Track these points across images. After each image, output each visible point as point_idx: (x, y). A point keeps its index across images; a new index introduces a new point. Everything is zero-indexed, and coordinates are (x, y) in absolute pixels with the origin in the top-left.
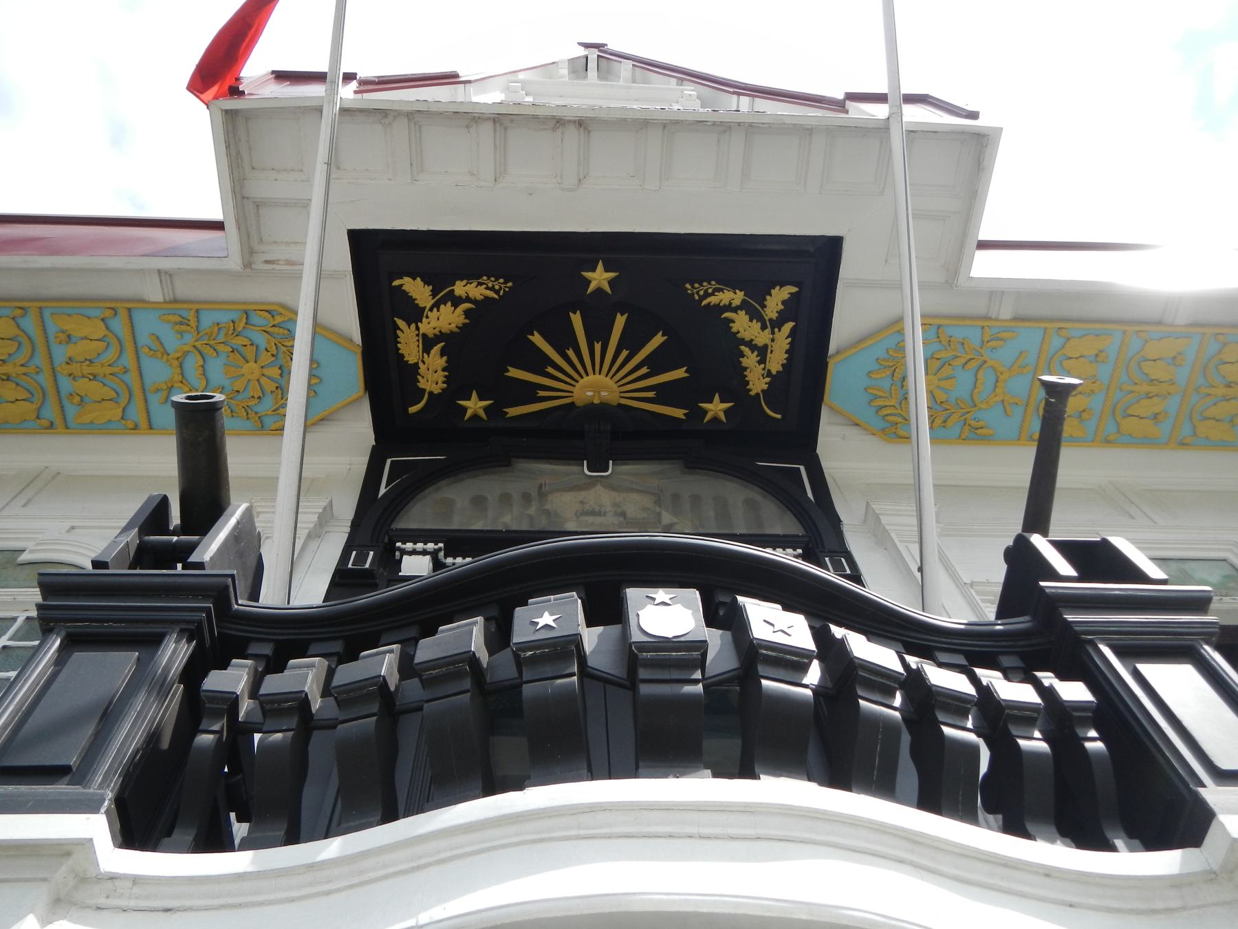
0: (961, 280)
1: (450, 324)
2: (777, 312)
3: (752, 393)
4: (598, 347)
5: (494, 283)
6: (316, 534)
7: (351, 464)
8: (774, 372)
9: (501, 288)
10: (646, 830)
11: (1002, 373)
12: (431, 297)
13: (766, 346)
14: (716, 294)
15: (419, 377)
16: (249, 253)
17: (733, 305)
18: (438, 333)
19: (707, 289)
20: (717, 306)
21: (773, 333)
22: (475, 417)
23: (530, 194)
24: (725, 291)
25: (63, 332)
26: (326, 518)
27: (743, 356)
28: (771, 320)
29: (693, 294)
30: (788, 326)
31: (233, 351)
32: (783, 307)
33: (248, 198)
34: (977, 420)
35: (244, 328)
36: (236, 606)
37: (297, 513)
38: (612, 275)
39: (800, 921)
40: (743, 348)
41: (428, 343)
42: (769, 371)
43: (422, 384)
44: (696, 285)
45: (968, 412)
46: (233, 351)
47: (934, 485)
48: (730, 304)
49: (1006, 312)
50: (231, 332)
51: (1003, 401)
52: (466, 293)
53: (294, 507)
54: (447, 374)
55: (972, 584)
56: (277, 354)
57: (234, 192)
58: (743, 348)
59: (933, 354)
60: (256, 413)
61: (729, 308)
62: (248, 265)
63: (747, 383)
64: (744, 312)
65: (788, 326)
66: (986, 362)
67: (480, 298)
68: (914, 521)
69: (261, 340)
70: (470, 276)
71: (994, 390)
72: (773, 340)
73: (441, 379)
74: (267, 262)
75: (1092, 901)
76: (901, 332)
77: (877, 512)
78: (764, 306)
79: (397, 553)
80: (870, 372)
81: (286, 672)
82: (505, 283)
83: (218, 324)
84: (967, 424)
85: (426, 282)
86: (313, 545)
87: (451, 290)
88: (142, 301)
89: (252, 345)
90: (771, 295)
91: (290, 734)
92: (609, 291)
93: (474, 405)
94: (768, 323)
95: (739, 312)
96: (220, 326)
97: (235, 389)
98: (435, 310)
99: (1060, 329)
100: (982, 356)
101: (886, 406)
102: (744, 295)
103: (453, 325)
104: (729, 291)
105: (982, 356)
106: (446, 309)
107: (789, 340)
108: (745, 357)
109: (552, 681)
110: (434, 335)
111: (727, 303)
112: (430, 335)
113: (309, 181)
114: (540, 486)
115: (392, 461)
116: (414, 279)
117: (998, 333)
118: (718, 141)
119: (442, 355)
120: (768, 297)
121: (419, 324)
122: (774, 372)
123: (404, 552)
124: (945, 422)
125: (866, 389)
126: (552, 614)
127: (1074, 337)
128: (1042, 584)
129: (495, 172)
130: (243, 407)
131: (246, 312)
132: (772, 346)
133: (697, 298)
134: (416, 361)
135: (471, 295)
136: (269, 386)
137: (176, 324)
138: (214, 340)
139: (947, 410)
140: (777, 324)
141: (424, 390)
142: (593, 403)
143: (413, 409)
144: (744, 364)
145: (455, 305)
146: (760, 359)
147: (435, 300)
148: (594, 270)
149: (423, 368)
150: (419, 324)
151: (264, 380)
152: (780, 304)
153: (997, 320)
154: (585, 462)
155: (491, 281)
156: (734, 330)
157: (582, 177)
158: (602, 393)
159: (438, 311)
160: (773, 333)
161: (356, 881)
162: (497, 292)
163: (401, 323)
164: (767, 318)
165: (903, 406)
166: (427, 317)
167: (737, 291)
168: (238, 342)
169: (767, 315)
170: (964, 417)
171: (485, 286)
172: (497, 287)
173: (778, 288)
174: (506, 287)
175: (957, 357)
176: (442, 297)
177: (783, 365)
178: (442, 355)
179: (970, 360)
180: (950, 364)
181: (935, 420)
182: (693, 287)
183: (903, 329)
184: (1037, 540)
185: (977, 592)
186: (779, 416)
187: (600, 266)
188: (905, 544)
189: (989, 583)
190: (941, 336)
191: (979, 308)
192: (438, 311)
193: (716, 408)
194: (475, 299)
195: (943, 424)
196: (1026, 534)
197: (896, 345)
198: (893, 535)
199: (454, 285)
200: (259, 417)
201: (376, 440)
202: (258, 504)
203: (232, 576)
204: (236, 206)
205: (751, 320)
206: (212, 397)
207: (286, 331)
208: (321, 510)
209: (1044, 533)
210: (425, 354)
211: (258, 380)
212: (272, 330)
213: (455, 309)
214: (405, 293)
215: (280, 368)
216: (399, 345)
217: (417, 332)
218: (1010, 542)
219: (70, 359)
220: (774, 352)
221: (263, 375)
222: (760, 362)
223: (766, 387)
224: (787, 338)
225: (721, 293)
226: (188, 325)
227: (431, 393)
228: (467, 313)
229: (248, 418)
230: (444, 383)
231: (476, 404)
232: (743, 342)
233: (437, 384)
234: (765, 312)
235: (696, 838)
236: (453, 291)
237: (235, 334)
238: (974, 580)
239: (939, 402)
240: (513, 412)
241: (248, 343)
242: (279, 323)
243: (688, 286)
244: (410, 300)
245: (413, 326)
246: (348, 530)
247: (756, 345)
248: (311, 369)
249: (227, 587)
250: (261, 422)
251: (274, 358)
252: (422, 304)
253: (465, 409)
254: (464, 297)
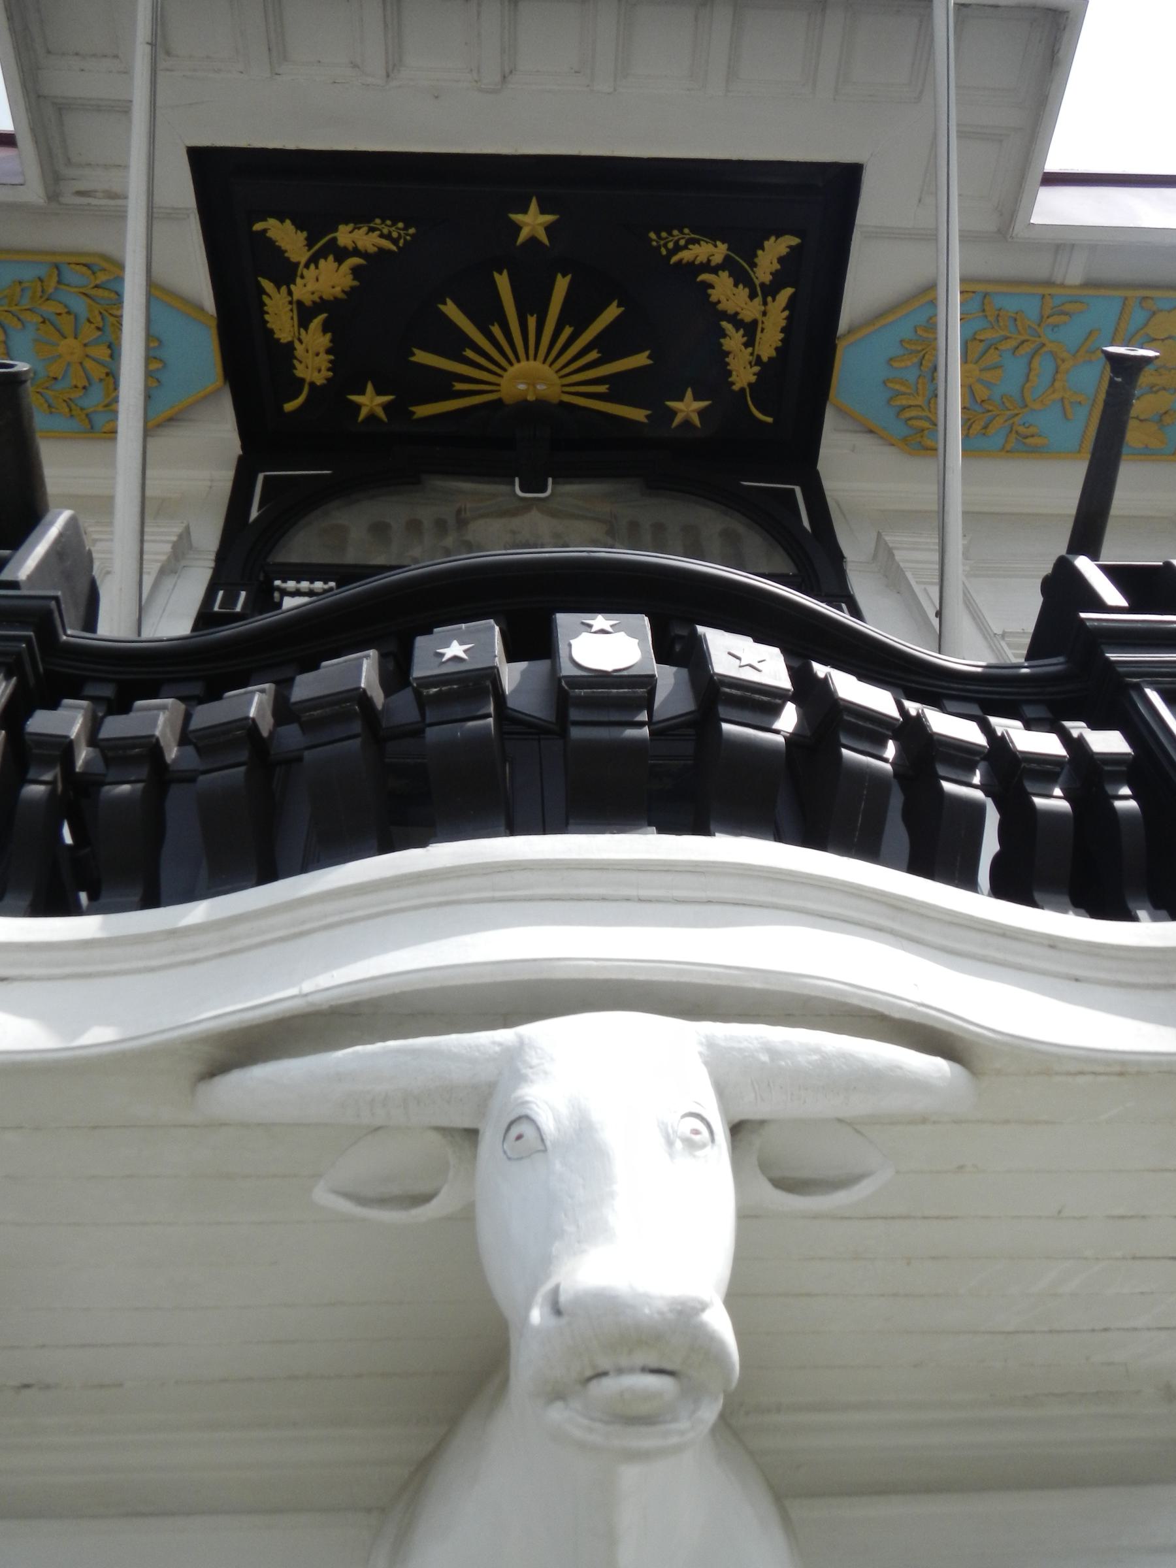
0: (1018, 228)
1: (333, 287)
2: (771, 274)
3: (736, 388)
4: (532, 321)
6: (169, 569)
7: (212, 480)
8: (765, 359)
9: (400, 236)
10: (574, 891)
11: (1063, 361)
12: (306, 248)
13: (755, 323)
14: (690, 246)
15: (295, 362)
16: (54, 179)
17: (713, 264)
18: (318, 300)
19: (679, 239)
20: (691, 264)
21: (765, 303)
22: (372, 417)
23: (437, 97)
24: (702, 243)
26: (182, 549)
27: (725, 335)
28: (762, 285)
29: (659, 247)
30: (786, 293)
31: (44, 322)
32: (778, 267)
33: (45, 97)
34: (1027, 425)
35: (56, 289)
36: (65, 638)
37: (142, 541)
38: (549, 218)
39: (754, 990)
40: (724, 324)
41: (305, 314)
42: (759, 357)
43: (300, 371)
44: (664, 234)
45: (1017, 415)
46: (44, 322)
47: (965, 513)
48: (709, 261)
49: (1074, 272)
50: (39, 294)
51: (1062, 399)
52: (354, 242)
53: (137, 527)
54: (332, 357)
55: (1004, 635)
56: (104, 326)
57: (24, 85)
58: (724, 324)
59: (975, 333)
60: (82, 409)
61: (707, 267)
62: (53, 196)
63: (730, 373)
64: (726, 274)
65: (786, 293)
66: (1044, 345)
67: (372, 250)
68: (936, 557)
69: (80, 306)
70: (360, 218)
71: (1053, 384)
72: (764, 314)
73: (325, 365)
74: (80, 193)
75: (1103, 975)
76: (933, 303)
77: (891, 545)
78: (753, 265)
79: (277, 595)
80: (891, 359)
81: (132, 714)
82: (406, 228)
83: (20, 283)
84: (1014, 432)
85: (299, 227)
86: (168, 582)
89: (69, 313)
90: (763, 250)
91: (140, 786)
92: (546, 241)
93: (370, 401)
94: (759, 289)
95: (720, 273)
96: (24, 285)
97: (52, 375)
98: (312, 266)
99: (1145, 298)
100: (1040, 337)
101: (910, 406)
102: (729, 249)
103: (338, 289)
104: (707, 242)
105: (1040, 337)
106: (327, 265)
107: (786, 313)
108: (728, 338)
109: (463, 724)
110: (314, 302)
111: (705, 261)
112: (308, 303)
113: (127, 72)
114: (459, 512)
115: (266, 477)
116: (282, 221)
117: (1063, 304)
118: (696, 19)
119: (325, 331)
120: (760, 252)
121: (292, 287)
122: (765, 359)
123: (285, 593)
124: (986, 427)
125: (884, 383)
126: (461, 643)
127: (1161, 311)
128: (1083, 615)
129: (387, 62)
130: (65, 401)
131: (57, 266)
132: (763, 322)
133: (664, 252)
134: (290, 339)
135: (360, 245)
136: (97, 372)
138: (16, 305)
139: (989, 411)
140: (770, 291)
141: (302, 381)
142: (526, 401)
143: (289, 407)
144: (725, 348)
145: (340, 260)
146: (747, 341)
148: (524, 210)
149: (299, 349)
150: (292, 287)
151: (88, 364)
152: (775, 261)
153: (1062, 286)
154: (517, 480)
155: (387, 225)
156: (714, 299)
157: (507, 70)
158: (539, 387)
159: (317, 267)
160: (765, 303)
161: (227, 948)
162: (395, 242)
163: (267, 285)
164: (757, 282)
165: (932, 405)
166: (302, 277)
167: (718, 243)
168: (50, 308)
169: (757, 278)
170: (1011, 421)
171: (378, 233)
172: (395, 235)
173: (773, 239)
174: (407, 235)
175: (1007, 338)
177: (777, 349)
178: (325, 331)
179: (1023, 342)
180: (996, 349)
181: (974, 425)
182: (659, 237)
183: (936, 299)
184: (1083, 563)
185: (1009, 645)
186: (769, 420)
187: (534, 206)
188: (923, 586)
189: (1024, 633)
190: (987, 308)
191: (1037, 267)
192: (317, 267)
193: (688, 408)
194: (366, 251)
195: (983, 431)
196: (1070, 557)
197: (928, 321)
198: (909, 575)
199: (336, 230)
200: (87, 415)
201: (243, 447)
202: (93, 529)
203: (56, 599)
204: (29, 109)
205: (736, 285)
206: (12, 366)
207: (113, 295)
208: (174, 538)
209: (1094, 556)
210: (302, 331)
211: (81, 363)
212: (94, 292)
214: (271, 242)
215: (110, 347)
216: (267, 317)
217: (290, 299)
218: (1048, 568)
220: (765, 331)
221: (87, 356)
222: (746, 345)
223: (753, 379)
224: (784, 310)
225: (697, 245)
227: (312, 385)
228: (356, 271)
229: (72, 416)
230: (329, 370)
231: (372, 401)
232: (724, 316)
233: (319, 371)
234: (754, 273)
235: (634, 901)
236: (335, 240)
238: (1006, 630)
239: (979, 401)
240: (423, 411)
241: (61, 309)
243: (652, 235)
244: (278, 253)
245: (284, 289)
246: (212, 564)
247: (742, 321)
248: (148, 348)
249: (50, 613)
250: (90, 421)
251: (99, 333)
252: (294, 258)
253: (358, 407)
254: (350, 248)
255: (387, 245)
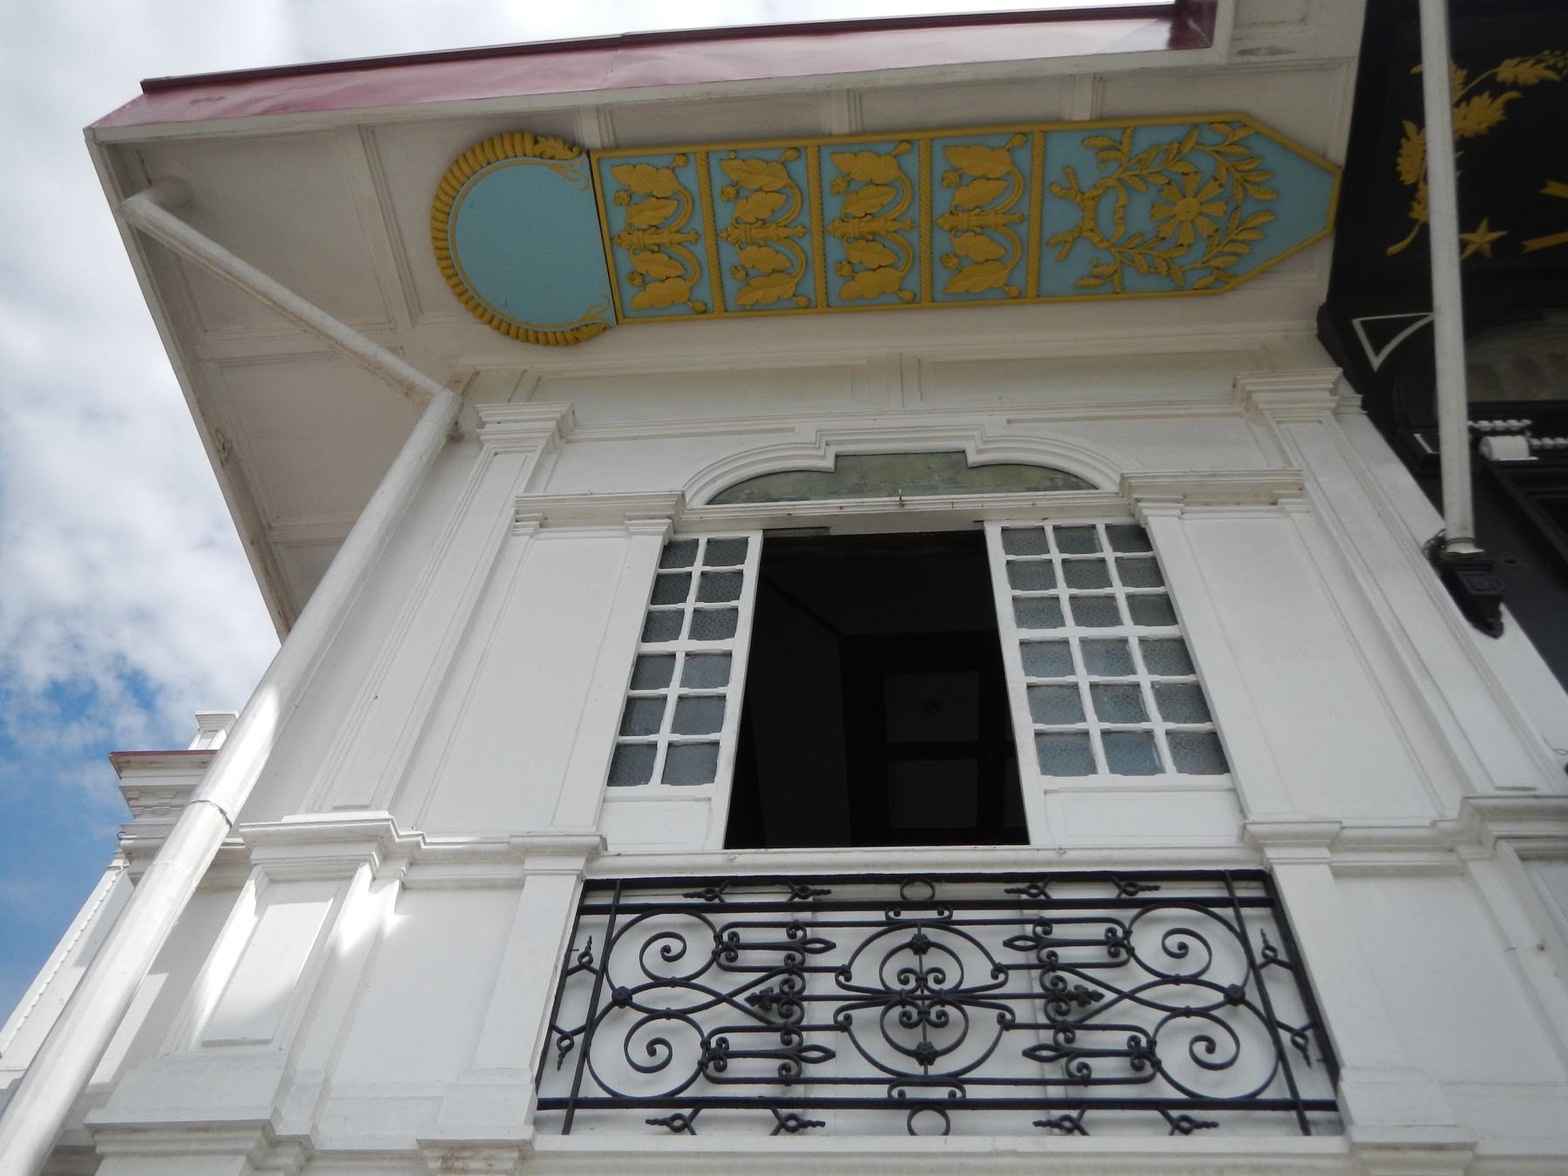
1: (1480, 124)
5: (1559, 59)
25: (956, 170)
31: (1169, 183)
35: (1192, 149)
70: (1526, 50)
87: (1489, 76)
88: (1059, 121)
89: (1196, 173)
103: (1484, 126)
130: (1165, 260)
137: (1103, 149)
143: (1393, 250)
145: (1494, 96)
147: (1467, 88)
171: (1543, 65)
176: (1476, 85)
192: (1468, 105)
202: (1246, 381)
213: (1492, 102)
219: (956, 207)
226: (1119, 150)
228: (1509, 105)
236: (1495, 75)
237: (1179, 158)
240: (1533, 245)
242: (1241, 139)
255: (1551, 75)
